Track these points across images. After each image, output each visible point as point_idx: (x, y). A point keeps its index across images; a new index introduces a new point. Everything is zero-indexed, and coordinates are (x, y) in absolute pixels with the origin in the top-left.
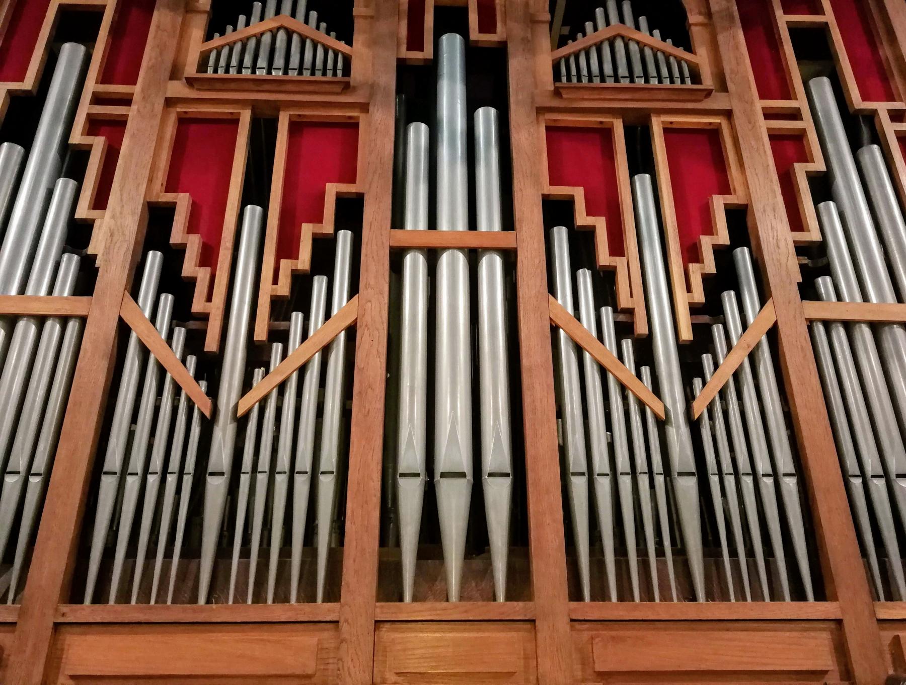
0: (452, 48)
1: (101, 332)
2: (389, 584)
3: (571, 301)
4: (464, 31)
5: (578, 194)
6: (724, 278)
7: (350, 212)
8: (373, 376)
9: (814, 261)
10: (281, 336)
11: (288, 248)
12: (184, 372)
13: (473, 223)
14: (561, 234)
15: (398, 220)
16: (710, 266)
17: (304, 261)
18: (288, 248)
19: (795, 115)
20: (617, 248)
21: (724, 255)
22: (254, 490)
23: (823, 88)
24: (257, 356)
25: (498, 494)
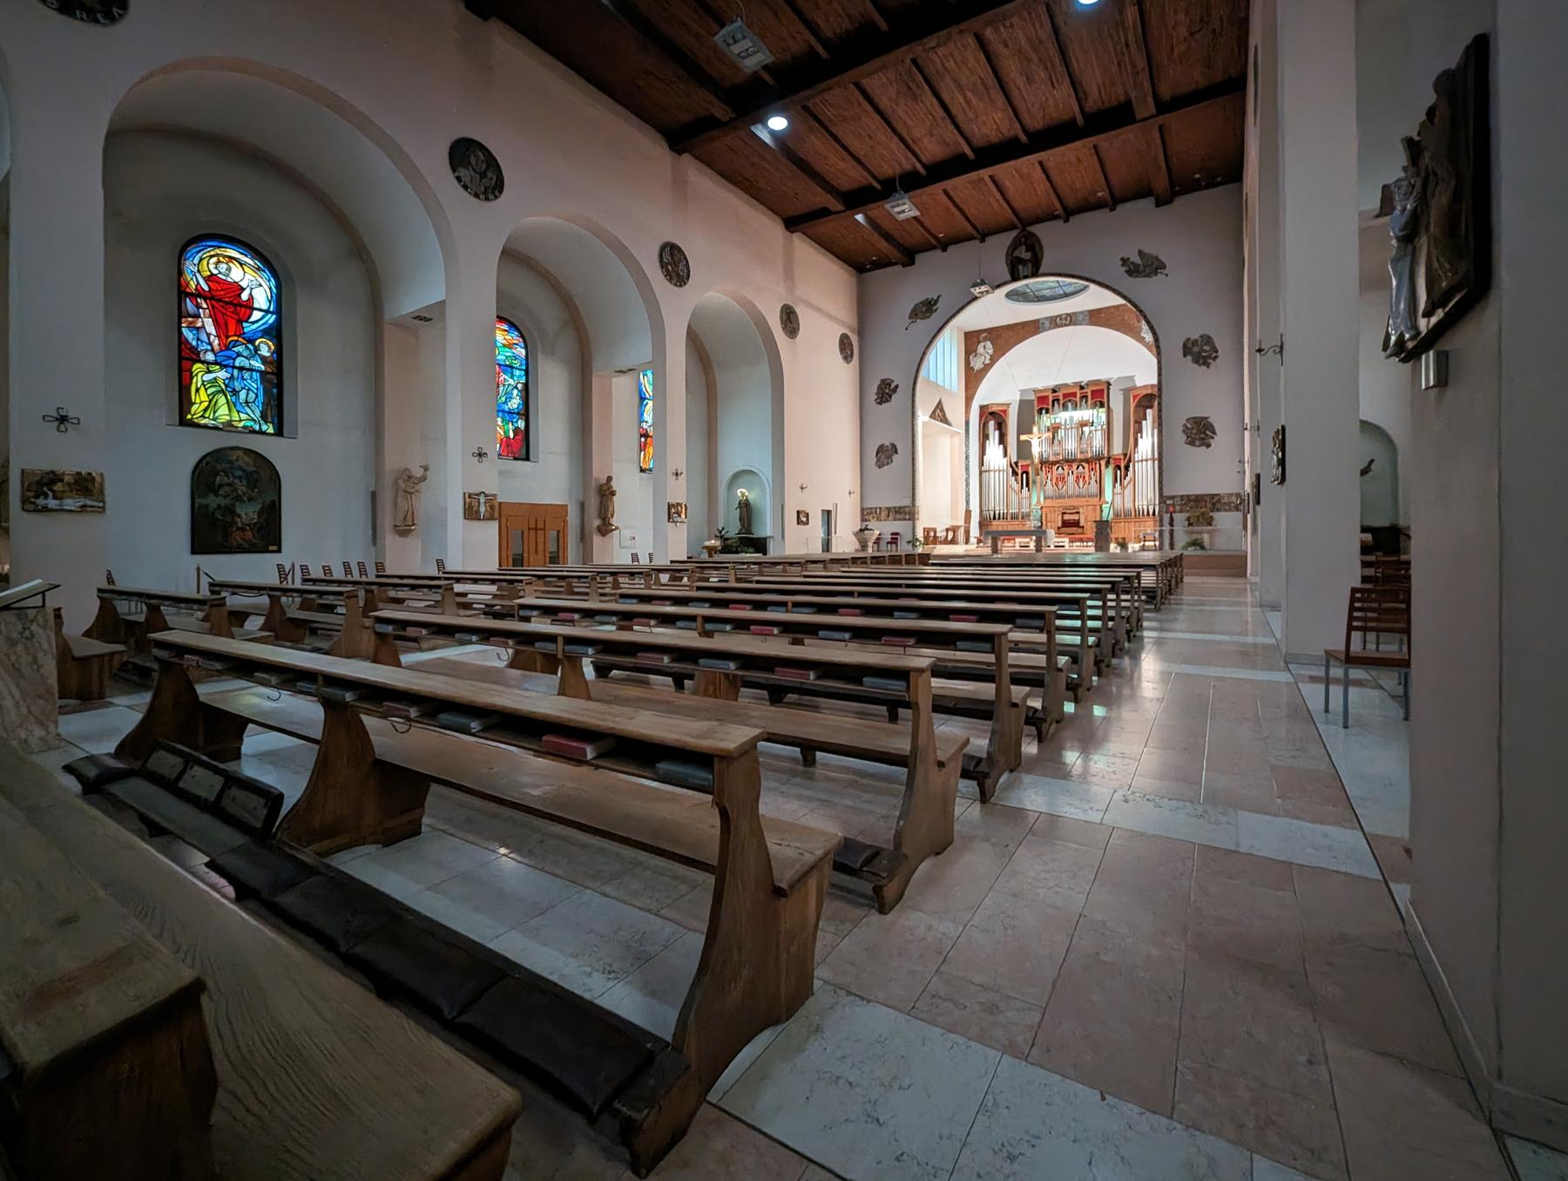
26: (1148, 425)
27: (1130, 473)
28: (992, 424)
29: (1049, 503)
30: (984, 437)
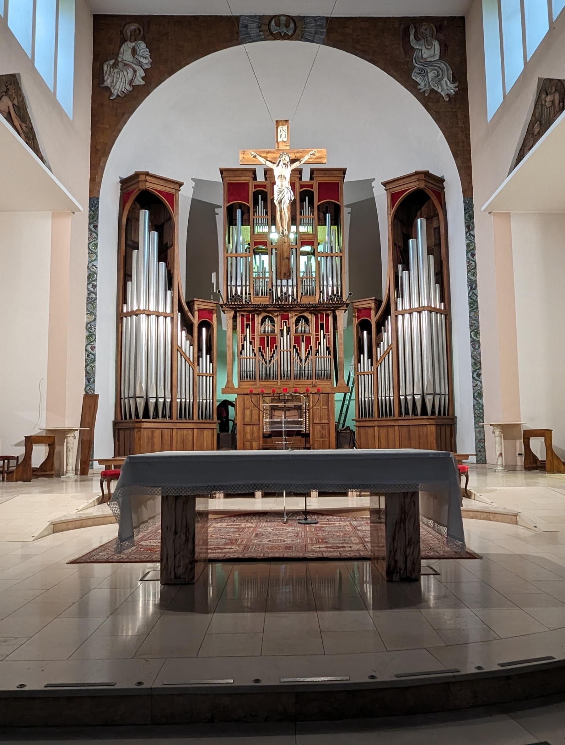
0: (285, 327)
1: (257, 360)
2: (281, 379)
4: (286, 325)
7: (276, 347)
9: (317, 351)
11: (271, 352)
18: (271, 352)
21: (309, 351)
22: (271, 372)
23: (322, 331)
24: (270, 362)
25: (289, 372)
26: (418, 246)
27: (387, 336)
28: (144, 215)
29: (248, 386)
30: (128, 244)
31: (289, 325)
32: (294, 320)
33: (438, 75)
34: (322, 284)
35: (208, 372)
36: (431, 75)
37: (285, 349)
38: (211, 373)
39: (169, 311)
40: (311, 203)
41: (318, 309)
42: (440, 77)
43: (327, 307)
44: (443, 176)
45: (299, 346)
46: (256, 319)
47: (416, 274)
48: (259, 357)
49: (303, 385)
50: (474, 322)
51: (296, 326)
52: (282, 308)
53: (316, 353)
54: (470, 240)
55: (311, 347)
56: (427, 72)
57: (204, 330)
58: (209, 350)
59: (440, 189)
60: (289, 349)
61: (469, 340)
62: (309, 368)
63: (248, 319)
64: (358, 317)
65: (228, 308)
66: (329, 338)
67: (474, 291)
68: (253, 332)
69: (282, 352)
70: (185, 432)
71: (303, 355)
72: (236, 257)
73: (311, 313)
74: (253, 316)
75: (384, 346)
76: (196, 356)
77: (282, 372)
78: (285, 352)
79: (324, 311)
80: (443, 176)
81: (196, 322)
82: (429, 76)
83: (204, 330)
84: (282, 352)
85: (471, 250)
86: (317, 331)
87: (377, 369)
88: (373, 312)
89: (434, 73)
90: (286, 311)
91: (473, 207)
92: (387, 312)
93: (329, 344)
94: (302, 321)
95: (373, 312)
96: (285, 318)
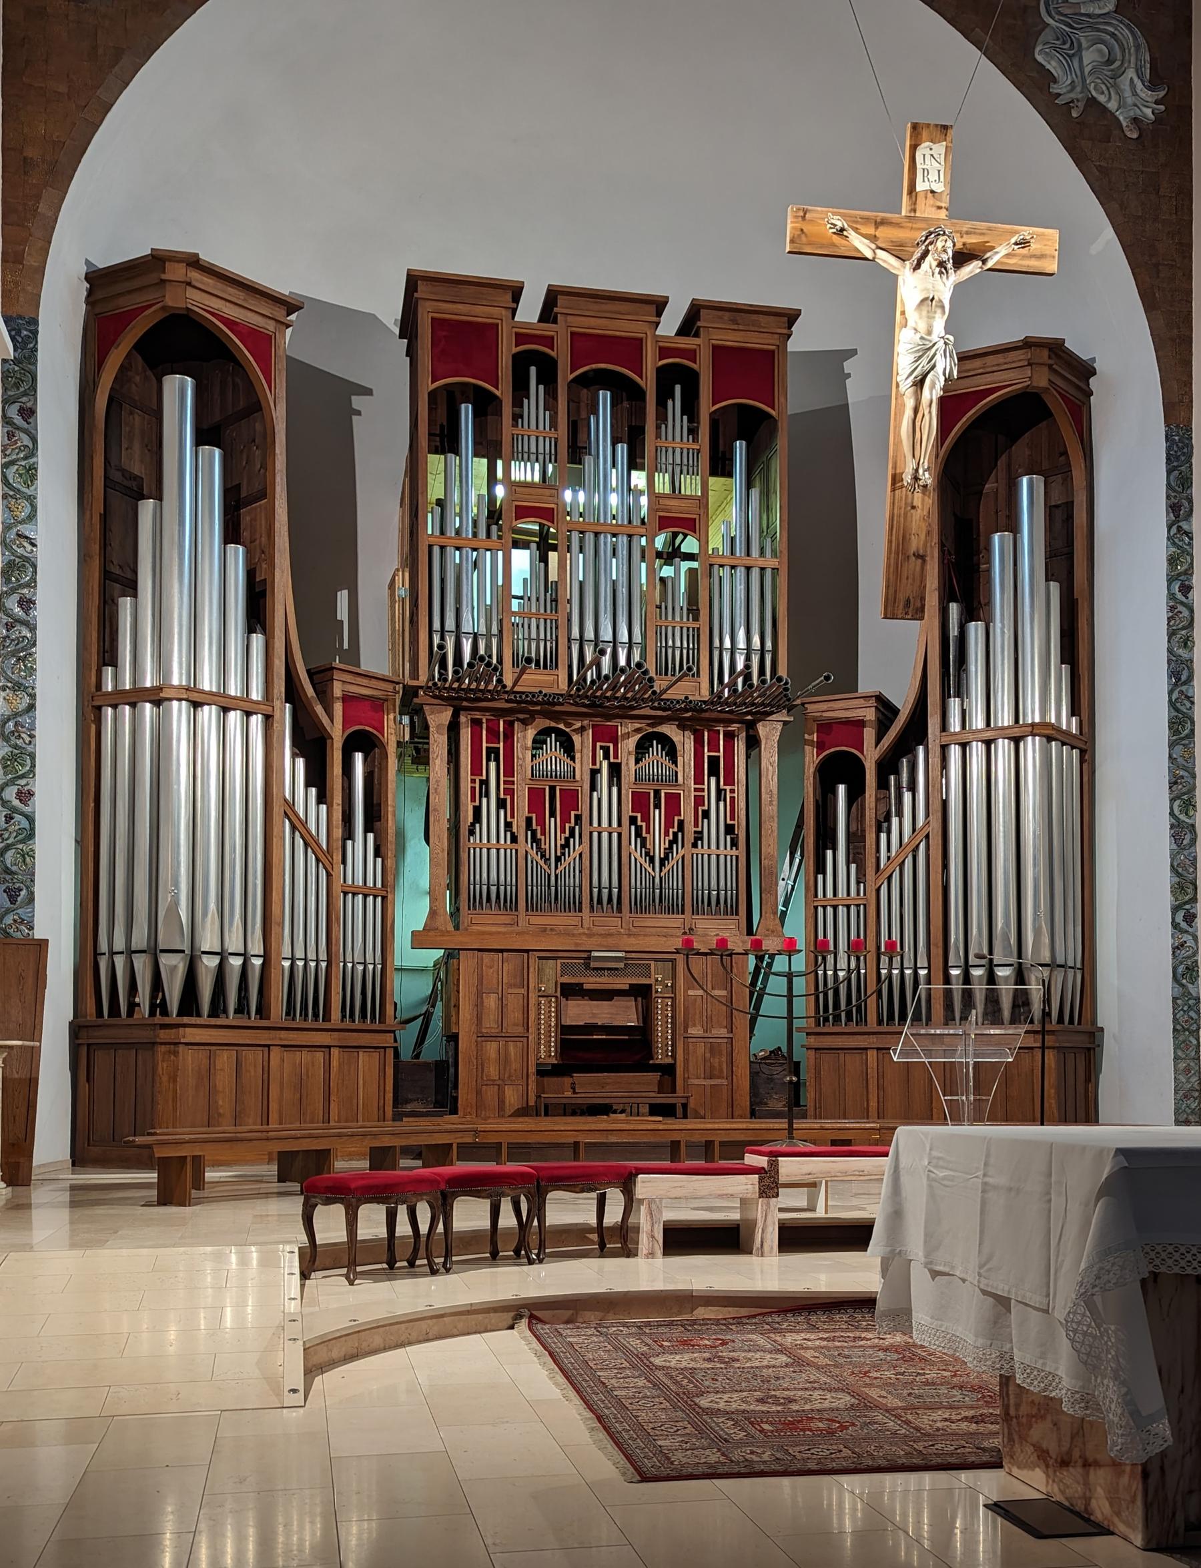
0: (605, 764)
3: (633, 848)
5: (639, 815)
6: (674, 841)
7: (578, 818)
8: (587, 865)
9: (699, 836)
10: (563, 854)
12: (542, 862)
13: (610, 824)
14: (633, 828)
15: (591, 824)
16: (671, 837)
17: (567, 834)
19: (703, 790)
20: (648, 832)
21: (675, 834)
23: (713, 780)
24: (558, 859)
26: (1016, 558)
31: (616, 757)
32: (631, 743)
33: (1110, 62)
34: (717, 643)
35: (370, 883)
36: (1090, 57)
37: (605, 823)
38: (379, 885)
39: (256, 694)
40: (690, 408)
41: (704, 715)
42: (1117, 64)
43: (731, 712)
44: (1094, 360)
45: (646, 818)
46: (517, 735)
47: (1009, 634)
48: (524, 845)
49: (661, 932)
50: (1182, 773)
51: (637, 762)
52: (600, 705)
53: (696, 839)
54: (1179, 547)
55: (681, 823)
56: (1080, 45)
57: (359, 757)
58: (374, 818)
59: (1080, 396)
60: (615, 824)
61: (1166, 821)
62: (676, 883)
63: (493, 735)
64: (821, 746)
65: (435, 697)
66: (732, 799)
67: (1184, 688)
68: (510, 771)
69: (595, 835)
70: (306, 1056)
71: (658, 843)
72: (442, 548)
73: (682, 727)
74: (510, 726)
75: (901, 828)
76: (338, 833)
77: (596, 890)
78: (605, 835)
79: (726, 719)
80: (1094, 360)
81: (337, 733)
82: (1085, 62)
83: (359, 757)
84: (595, 835)
85: (1179, 574)
86: (699, 779)
87: (878, 891)
88: (869, 734)
89: (1100, 51)
90: (609, 717)
91: (1191, 456)
92: (916, 732)
93: (732, 818)
94: (656, 750)
95: (869, 734)
96: (606, 737)
